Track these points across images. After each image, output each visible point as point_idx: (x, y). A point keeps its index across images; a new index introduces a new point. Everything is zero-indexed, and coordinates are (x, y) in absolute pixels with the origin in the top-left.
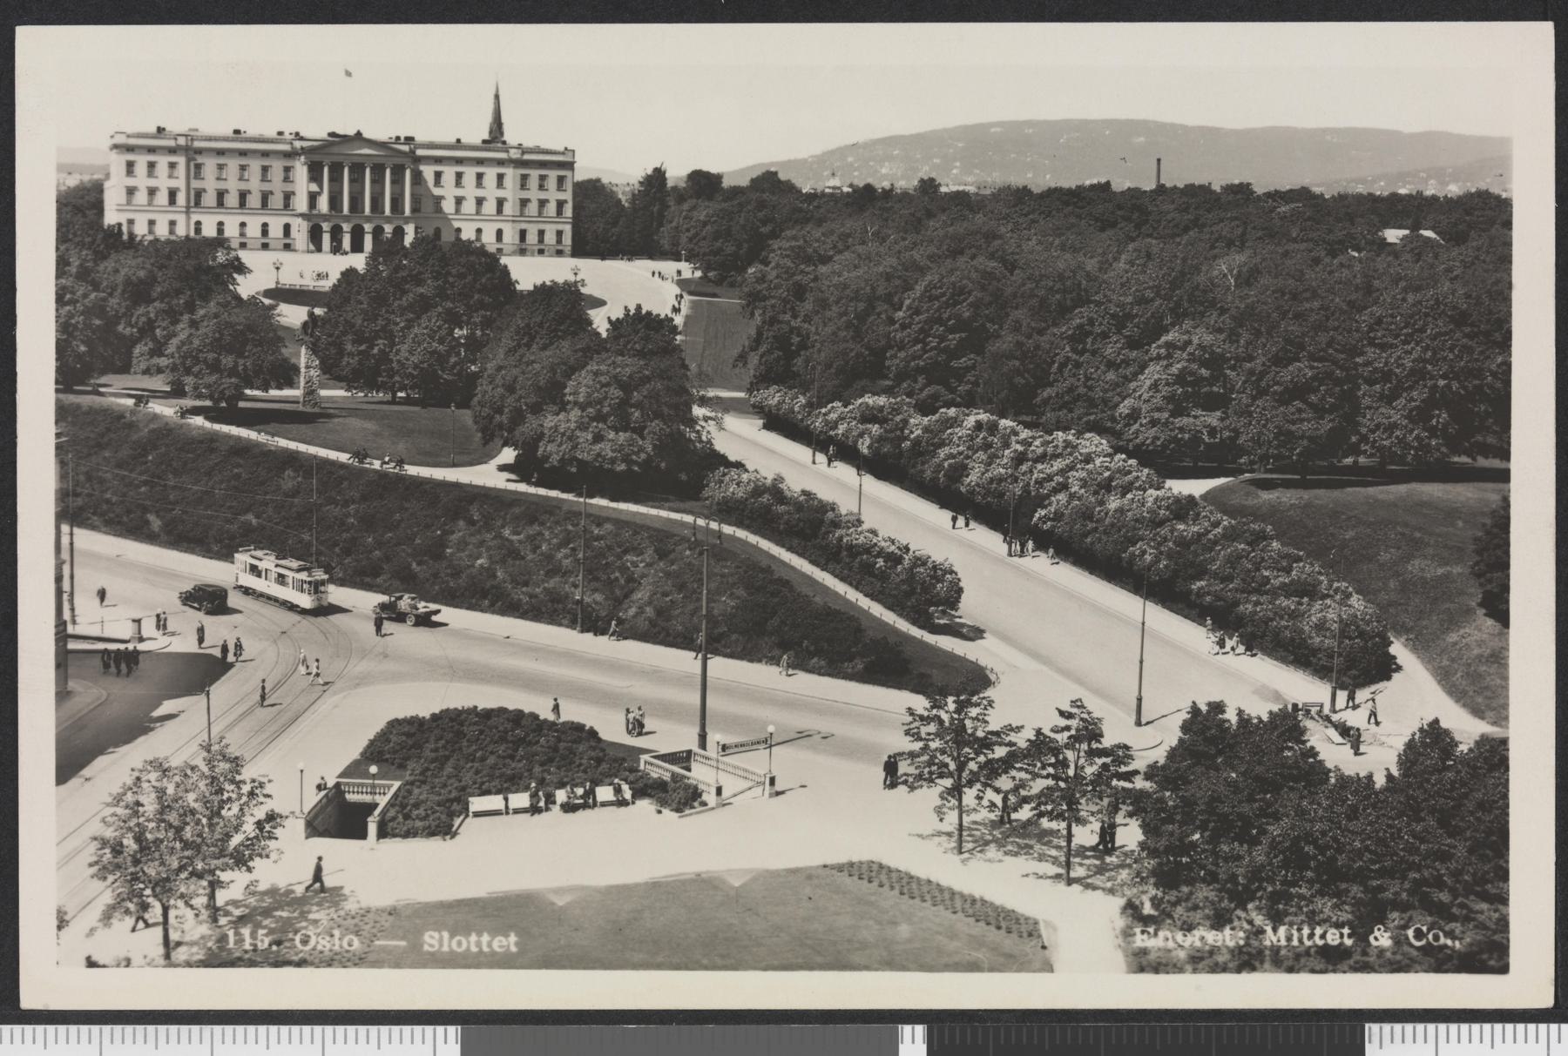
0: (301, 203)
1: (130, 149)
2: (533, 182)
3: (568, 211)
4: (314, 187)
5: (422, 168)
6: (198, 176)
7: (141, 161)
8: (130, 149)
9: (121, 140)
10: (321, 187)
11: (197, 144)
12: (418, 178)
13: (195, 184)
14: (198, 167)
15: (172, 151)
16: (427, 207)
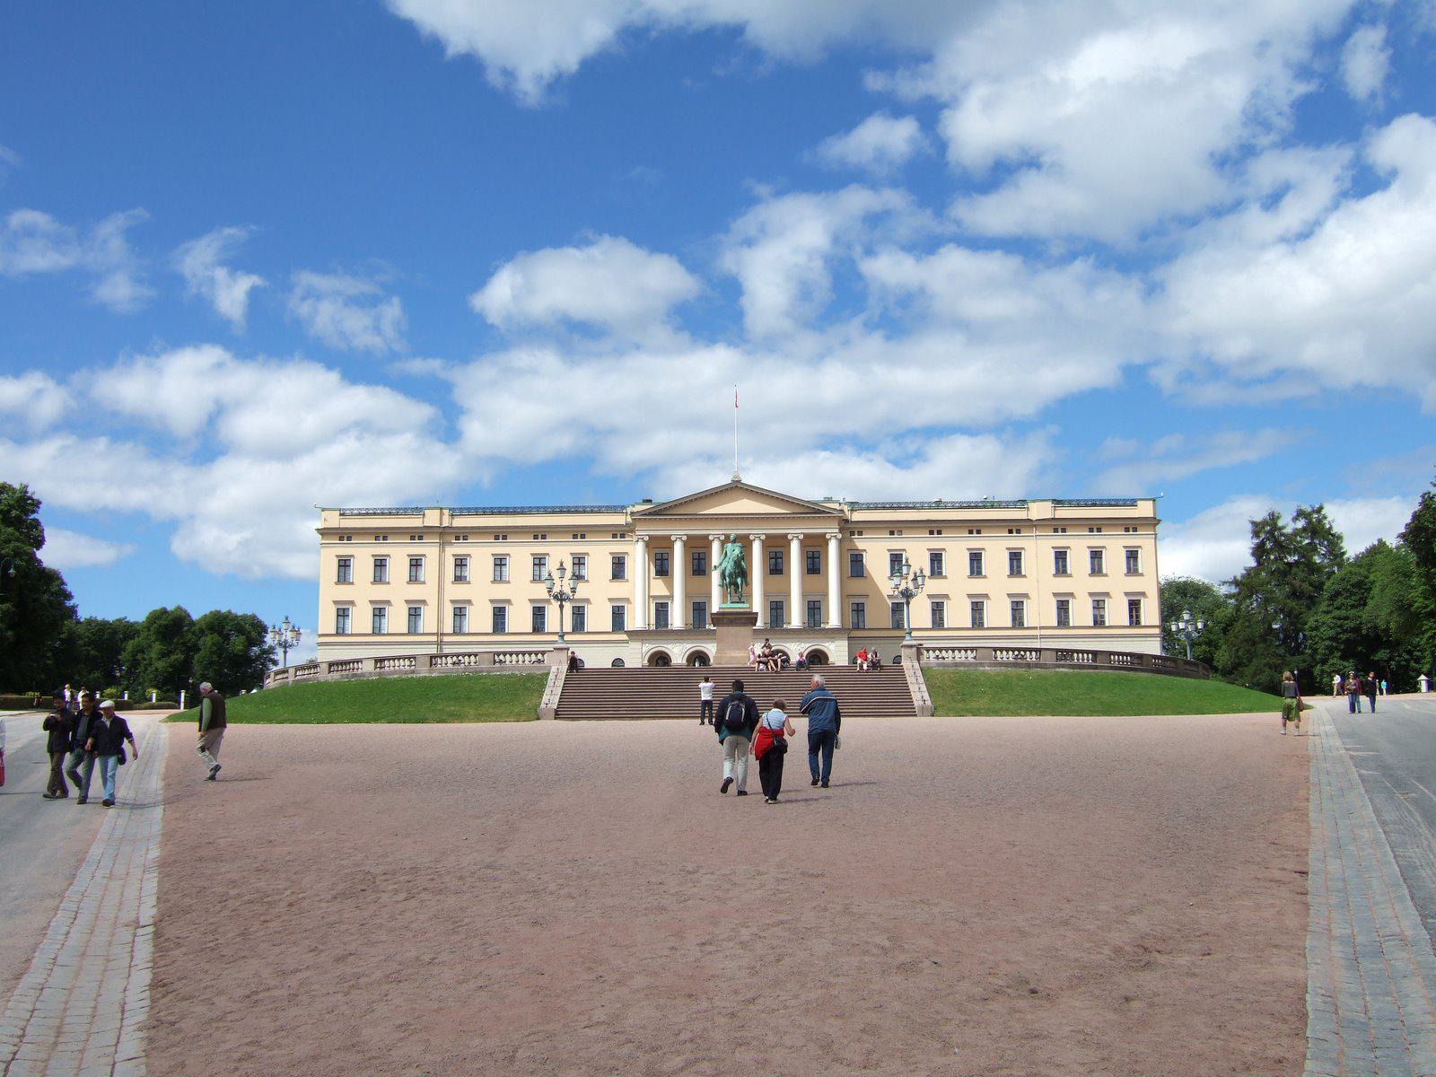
0: (637, 618)
1: (345, 535)
2: (1079, 560)
3: (1151, 612)
4: (659, 587)
5: (860, 544)
7: (363, 555)
8: (345, 535)
9: (334, 521)
10: (670, 586)
11: (460, 522)
12: (855, 566)
13: (456, 592)
14: (460, 563)
15: (417, 535)
16: (877, 617)
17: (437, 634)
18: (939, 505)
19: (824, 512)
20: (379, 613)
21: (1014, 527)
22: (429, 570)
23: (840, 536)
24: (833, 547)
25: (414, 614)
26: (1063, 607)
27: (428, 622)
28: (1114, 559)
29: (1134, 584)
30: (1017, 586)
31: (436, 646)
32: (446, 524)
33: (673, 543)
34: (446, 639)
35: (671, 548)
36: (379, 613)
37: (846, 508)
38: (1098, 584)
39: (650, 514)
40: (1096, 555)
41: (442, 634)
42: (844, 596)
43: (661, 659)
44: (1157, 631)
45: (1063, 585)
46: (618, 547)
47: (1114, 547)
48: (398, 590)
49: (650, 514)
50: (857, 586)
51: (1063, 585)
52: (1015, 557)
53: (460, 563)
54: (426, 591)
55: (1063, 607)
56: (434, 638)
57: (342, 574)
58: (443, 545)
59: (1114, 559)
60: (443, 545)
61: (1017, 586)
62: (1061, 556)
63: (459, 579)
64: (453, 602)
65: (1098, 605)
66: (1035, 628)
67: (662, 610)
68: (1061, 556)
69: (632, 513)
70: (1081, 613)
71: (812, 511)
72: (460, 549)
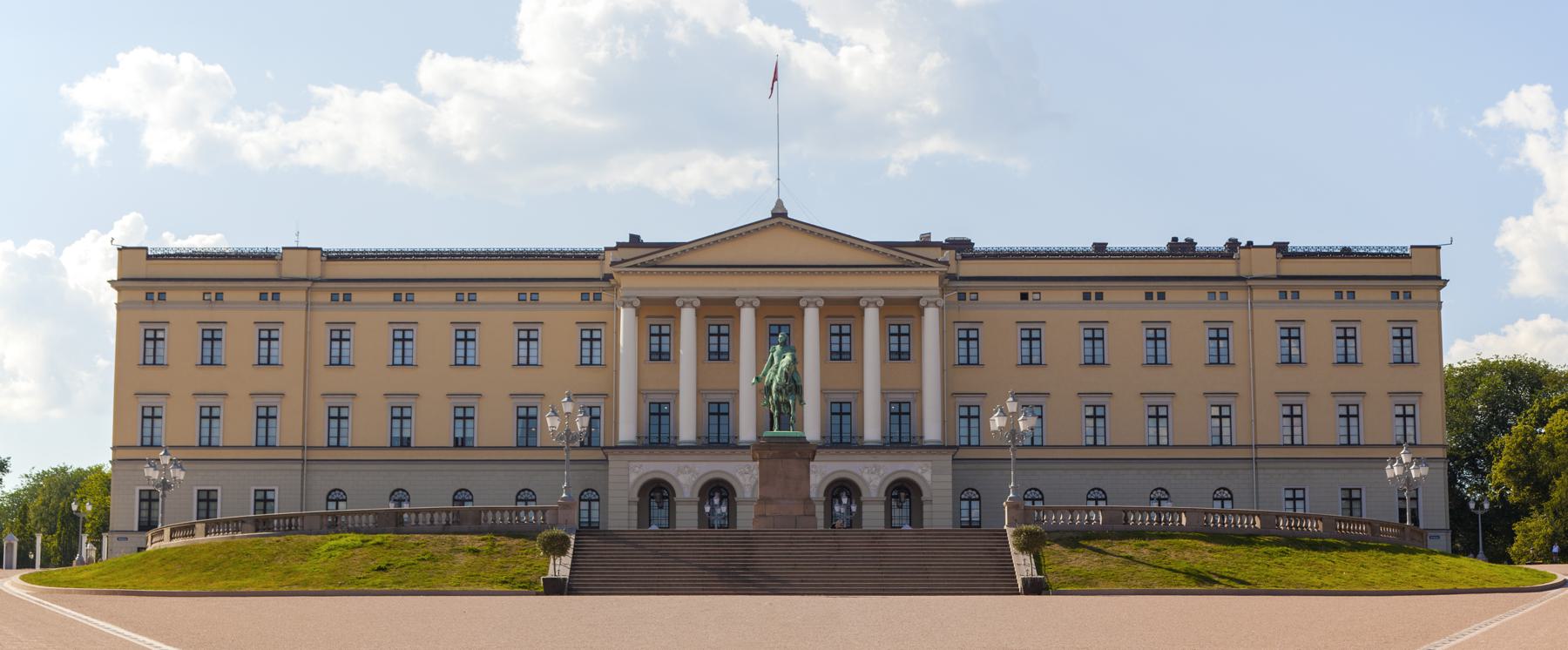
2: (1319, 340)
3: (1433, 427)
14: (339, 336)
17: (302, 447)
18: (1100, 250)
19: (917, 265)
20: (209, 416)
22: (288, 349)
23: (941, 302)
24: (931, 316)
25: (266, 417)
27: (287, 430)
28: (1376, 341)
29: (1404, 379)
30: (1221, 379)
31: (299, 467)
32: (316, 274)
33: (679, 310)
35: (676, 316)
36: (209, 416)
37: (948, 255)
38: (1349, 379)
39: (644, 265)
42: (949, 395)
43: (657, 492)
44: (1441, 453)
45: (1292, 379)
46: (591, 313)
47: (1375, 317)
48: (239, 377)
49: (644, 265)
50: (969, 380)
51: (1292, 379)
52: (1220, 335)
53: (339, 336)
54: (284, 379)
56: (297, 454)
57: (150, 352)
59: (1376, 341)
60: (309, 306)
61: (1221, 379)
62: (1291, 334)
63: (338, 362)
67: (659, 413)
68: (1291, 334)
69: (613, 264)
71: (901, 255)
72: (341, 314)
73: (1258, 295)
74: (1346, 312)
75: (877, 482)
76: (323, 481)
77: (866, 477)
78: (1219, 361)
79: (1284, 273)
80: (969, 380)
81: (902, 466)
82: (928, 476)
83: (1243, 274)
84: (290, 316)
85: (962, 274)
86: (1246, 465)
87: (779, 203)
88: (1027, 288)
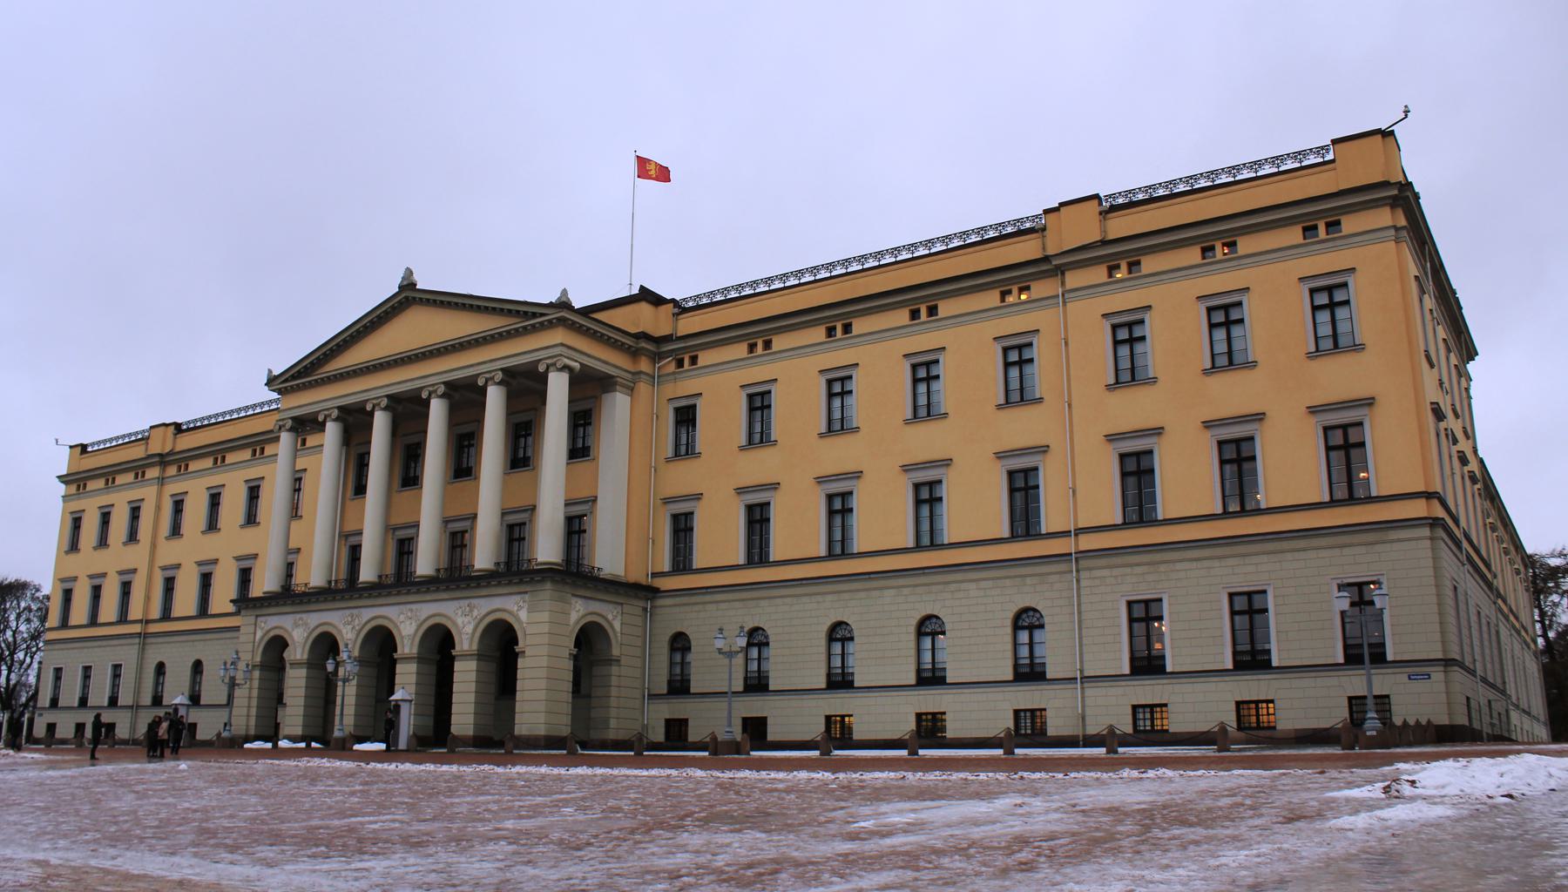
6: (176, 531)
11: (186, 442)
17: (140, 621)
19: (534, 315)
21: (1008, 280)
26: (1137, 472)
30: (1022, 427)
34: (153, 628)
38: (1232, 395)
39: (293, 377)
40: (1224, 316)
41: (148, 622)
45: (1134, 409)
50: (682, 477)
51: (1134, 409)
52: (1017, 355)
55: (1137, 472)
56: (137, 628)
58: (162, 481)
62: (1127, 332)
64: (164, 568)
65: (1237, 459)
66: (1066, 534)
68: (1127, 332)
70: (1188, 482)
73: (1074, 279)
74: (1219, 281)
75: (469, 629)
76: (153, 657)
77: (460, 621)
78: (1018, 396)
79: (1111, 237)
80: (682, 477)
81: (497, 603)
82: (523, 615)
83: (1050, 252)
84: (148, 493)
85: (681, 332)
86: (1062, 567)
87: (409, 272)
88: (758, 334)
